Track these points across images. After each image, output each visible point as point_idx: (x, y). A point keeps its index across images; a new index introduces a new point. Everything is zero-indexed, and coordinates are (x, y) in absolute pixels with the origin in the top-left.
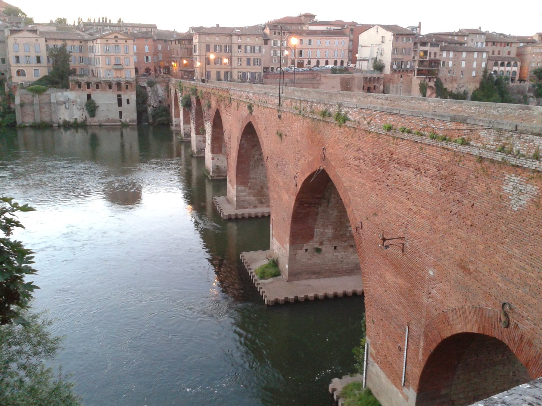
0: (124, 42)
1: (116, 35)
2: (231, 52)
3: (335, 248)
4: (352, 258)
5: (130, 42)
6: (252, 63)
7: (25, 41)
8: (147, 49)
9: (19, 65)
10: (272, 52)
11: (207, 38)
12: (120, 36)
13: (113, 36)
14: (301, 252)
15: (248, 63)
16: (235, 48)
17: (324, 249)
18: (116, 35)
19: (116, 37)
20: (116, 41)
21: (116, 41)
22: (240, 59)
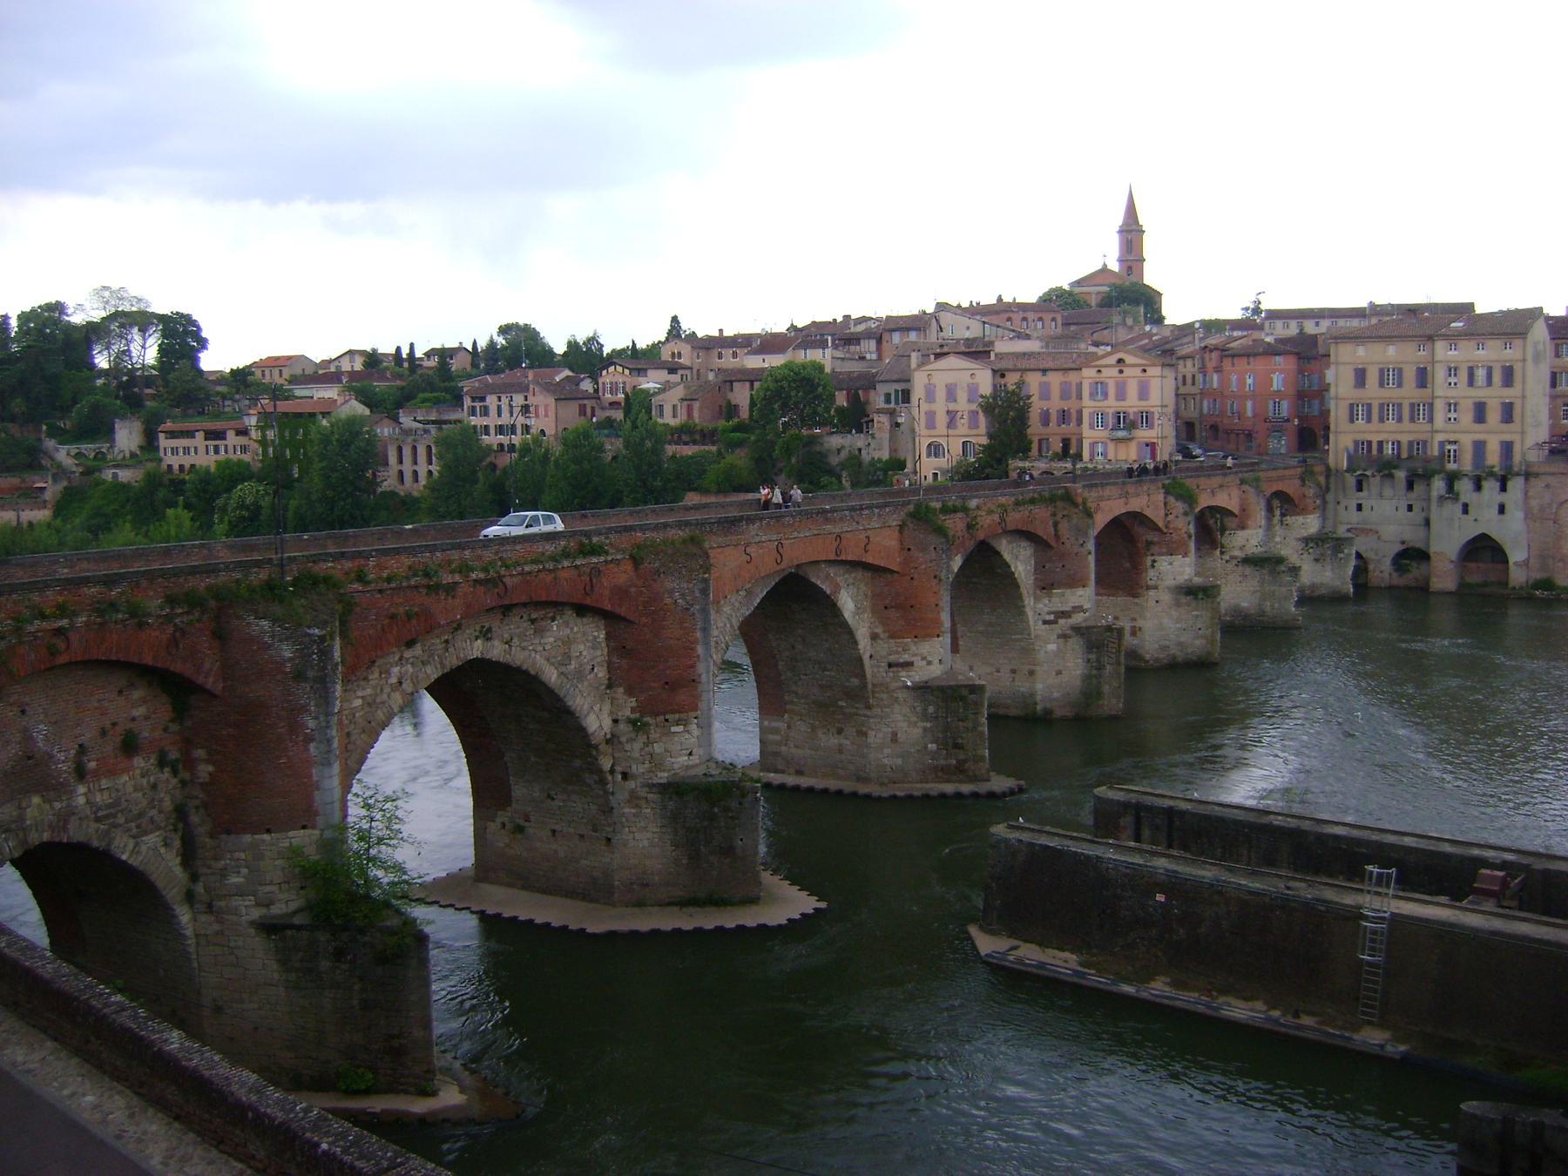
0: (1137, 372)
1: (1120, 355)
3: (554, 831)
4: (584, 862)
5: (1155, 371)
7: (949, 378)
8: (1277, 382)
9: (933, 432)
11: (1361, 351)
12: (1129, 359)
13: (1112, 360)
14: (493, 827)
16: (1440, 374)
17: (531, 831)
18: (1120, 355)
19: (1120, 361)
20: (1121, 372)
21: (1121, 372)
22: (1452, 406)
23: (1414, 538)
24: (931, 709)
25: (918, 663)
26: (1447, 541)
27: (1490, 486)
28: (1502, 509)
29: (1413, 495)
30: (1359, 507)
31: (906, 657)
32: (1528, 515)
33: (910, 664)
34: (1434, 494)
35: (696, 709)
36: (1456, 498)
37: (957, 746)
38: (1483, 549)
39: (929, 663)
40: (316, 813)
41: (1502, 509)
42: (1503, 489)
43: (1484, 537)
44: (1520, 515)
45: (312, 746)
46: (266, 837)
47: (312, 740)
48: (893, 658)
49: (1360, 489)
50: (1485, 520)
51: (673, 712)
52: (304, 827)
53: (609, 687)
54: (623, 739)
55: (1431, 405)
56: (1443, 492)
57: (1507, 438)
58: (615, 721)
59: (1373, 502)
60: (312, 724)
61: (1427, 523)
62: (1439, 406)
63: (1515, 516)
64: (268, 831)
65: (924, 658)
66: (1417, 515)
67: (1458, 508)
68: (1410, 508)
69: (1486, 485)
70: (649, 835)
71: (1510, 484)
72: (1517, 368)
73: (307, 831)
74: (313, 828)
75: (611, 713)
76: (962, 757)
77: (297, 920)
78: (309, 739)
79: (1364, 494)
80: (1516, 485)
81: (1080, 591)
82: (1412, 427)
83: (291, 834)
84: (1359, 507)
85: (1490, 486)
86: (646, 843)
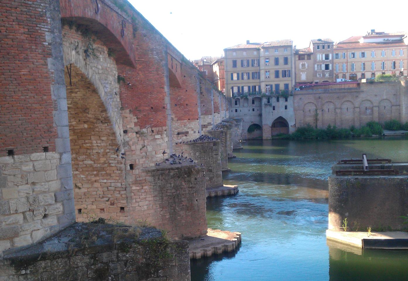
2: (259, 65)
6: (281, 75)
10: (316, 66)
15: (277, 76)
23: (256, 121)
24: (197, 154)
25: (191, 132)
26: (268, 120)
27: (282, 100)
28: (286, 108)
29: (254, 105)
30: (236, 111)
31: (185, 130)
32: (295, 110)
33: (187, 133)
34: (263, 103)
35: (165, 125)
36: (270, 105)
37: (211, 171)
38: (281, 122)
39: (195, 132)
40: (56, 136)
41: (286, 108)
42: (286, 100)
43: (280, 118)
44: (292, 109)
45: (50, 60)
46: (8, 159)
47: (50, 55)
48: (180, 130)
49: (236, 104)
50: (280, 112)
51: (156, 126)
52: (46, 149)
53: (122, 109)
54: (131, 143)
55: (259, 73)
56: (266, 103)
57: (286, 82)
58: (125, 132)
59: (241, 109)
60: (48, 37)
61: (260, 115)
62: (262, 72)
63: (290, 109)
64: (11, 153)
65: (193, 130)
66: (256, 112)
67: (272, 108)
68: (253, 110)
69: (280, 99)
70: (147, 202)
71: (288, 100)
72: (289, 58)
73: (49, 154)
74: (54, 150)
75: (123, 126)
76: (212, 176)
77: (48, 248)
78: (47, 54)
79: (238, 105)
80: (290, 99)
81: (210, 116)
82: (253, 81)
83: (35, 156)
84: (236, 111)
85: (282, 100)
86: (145, 207)
